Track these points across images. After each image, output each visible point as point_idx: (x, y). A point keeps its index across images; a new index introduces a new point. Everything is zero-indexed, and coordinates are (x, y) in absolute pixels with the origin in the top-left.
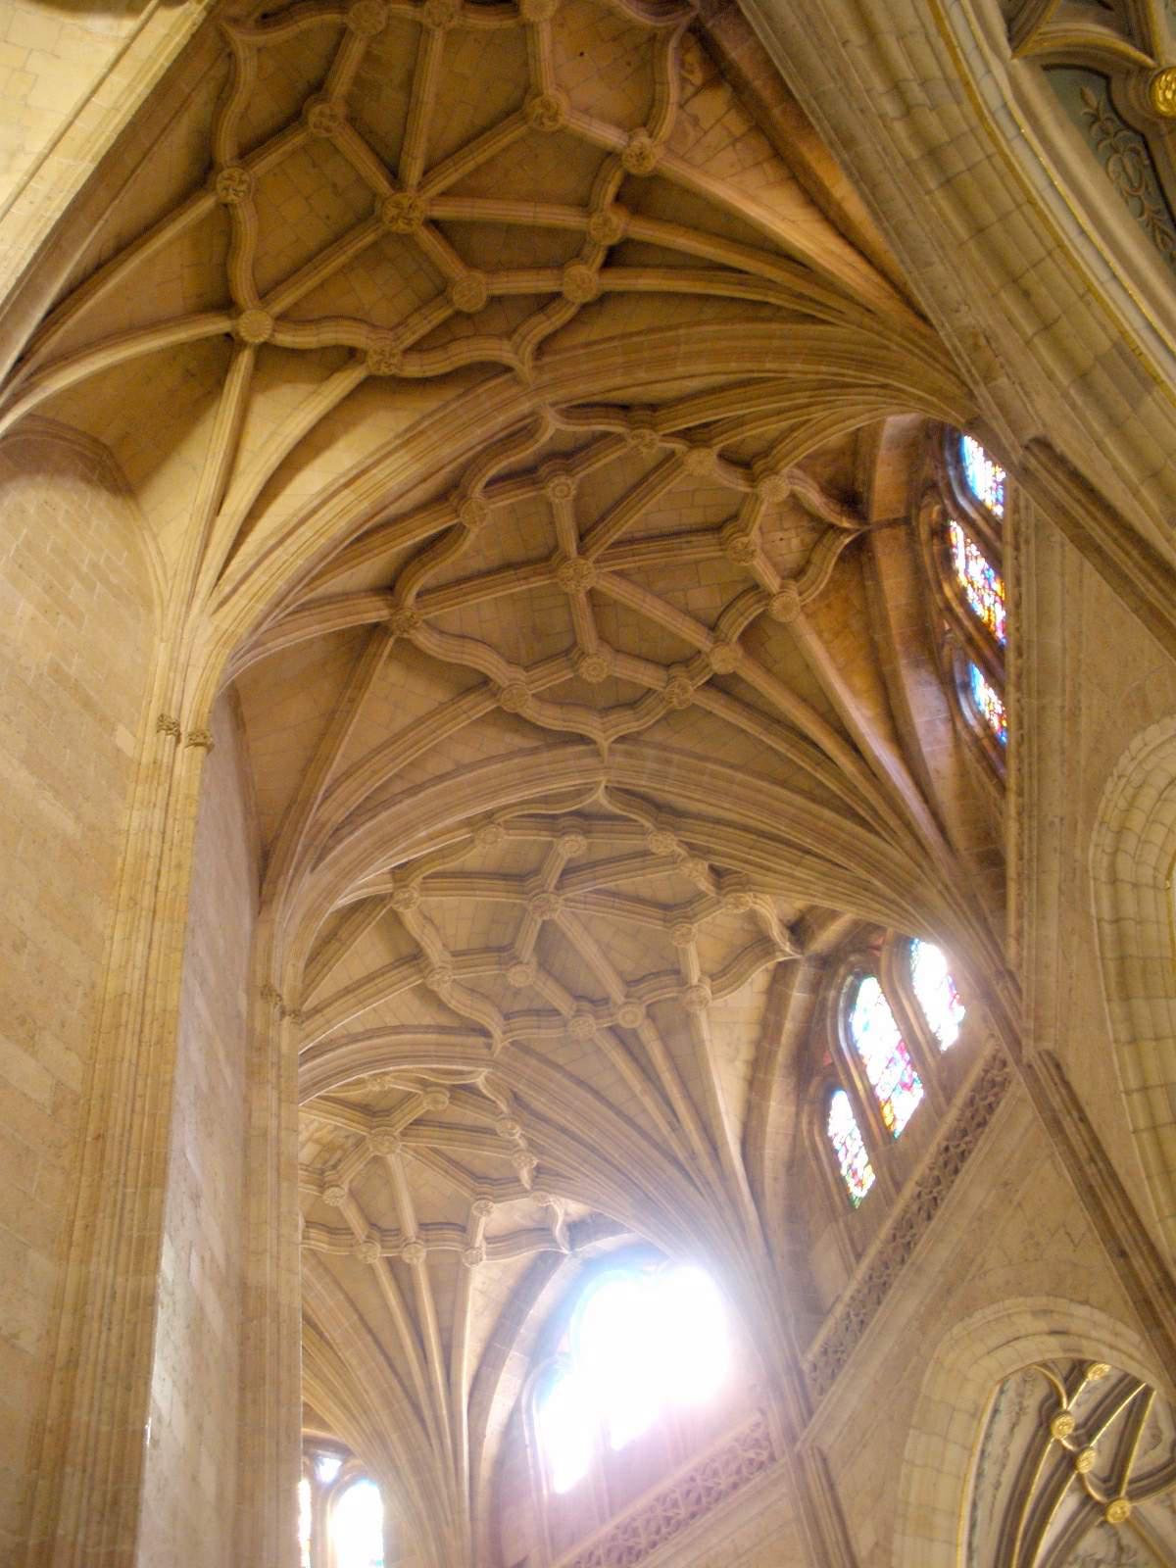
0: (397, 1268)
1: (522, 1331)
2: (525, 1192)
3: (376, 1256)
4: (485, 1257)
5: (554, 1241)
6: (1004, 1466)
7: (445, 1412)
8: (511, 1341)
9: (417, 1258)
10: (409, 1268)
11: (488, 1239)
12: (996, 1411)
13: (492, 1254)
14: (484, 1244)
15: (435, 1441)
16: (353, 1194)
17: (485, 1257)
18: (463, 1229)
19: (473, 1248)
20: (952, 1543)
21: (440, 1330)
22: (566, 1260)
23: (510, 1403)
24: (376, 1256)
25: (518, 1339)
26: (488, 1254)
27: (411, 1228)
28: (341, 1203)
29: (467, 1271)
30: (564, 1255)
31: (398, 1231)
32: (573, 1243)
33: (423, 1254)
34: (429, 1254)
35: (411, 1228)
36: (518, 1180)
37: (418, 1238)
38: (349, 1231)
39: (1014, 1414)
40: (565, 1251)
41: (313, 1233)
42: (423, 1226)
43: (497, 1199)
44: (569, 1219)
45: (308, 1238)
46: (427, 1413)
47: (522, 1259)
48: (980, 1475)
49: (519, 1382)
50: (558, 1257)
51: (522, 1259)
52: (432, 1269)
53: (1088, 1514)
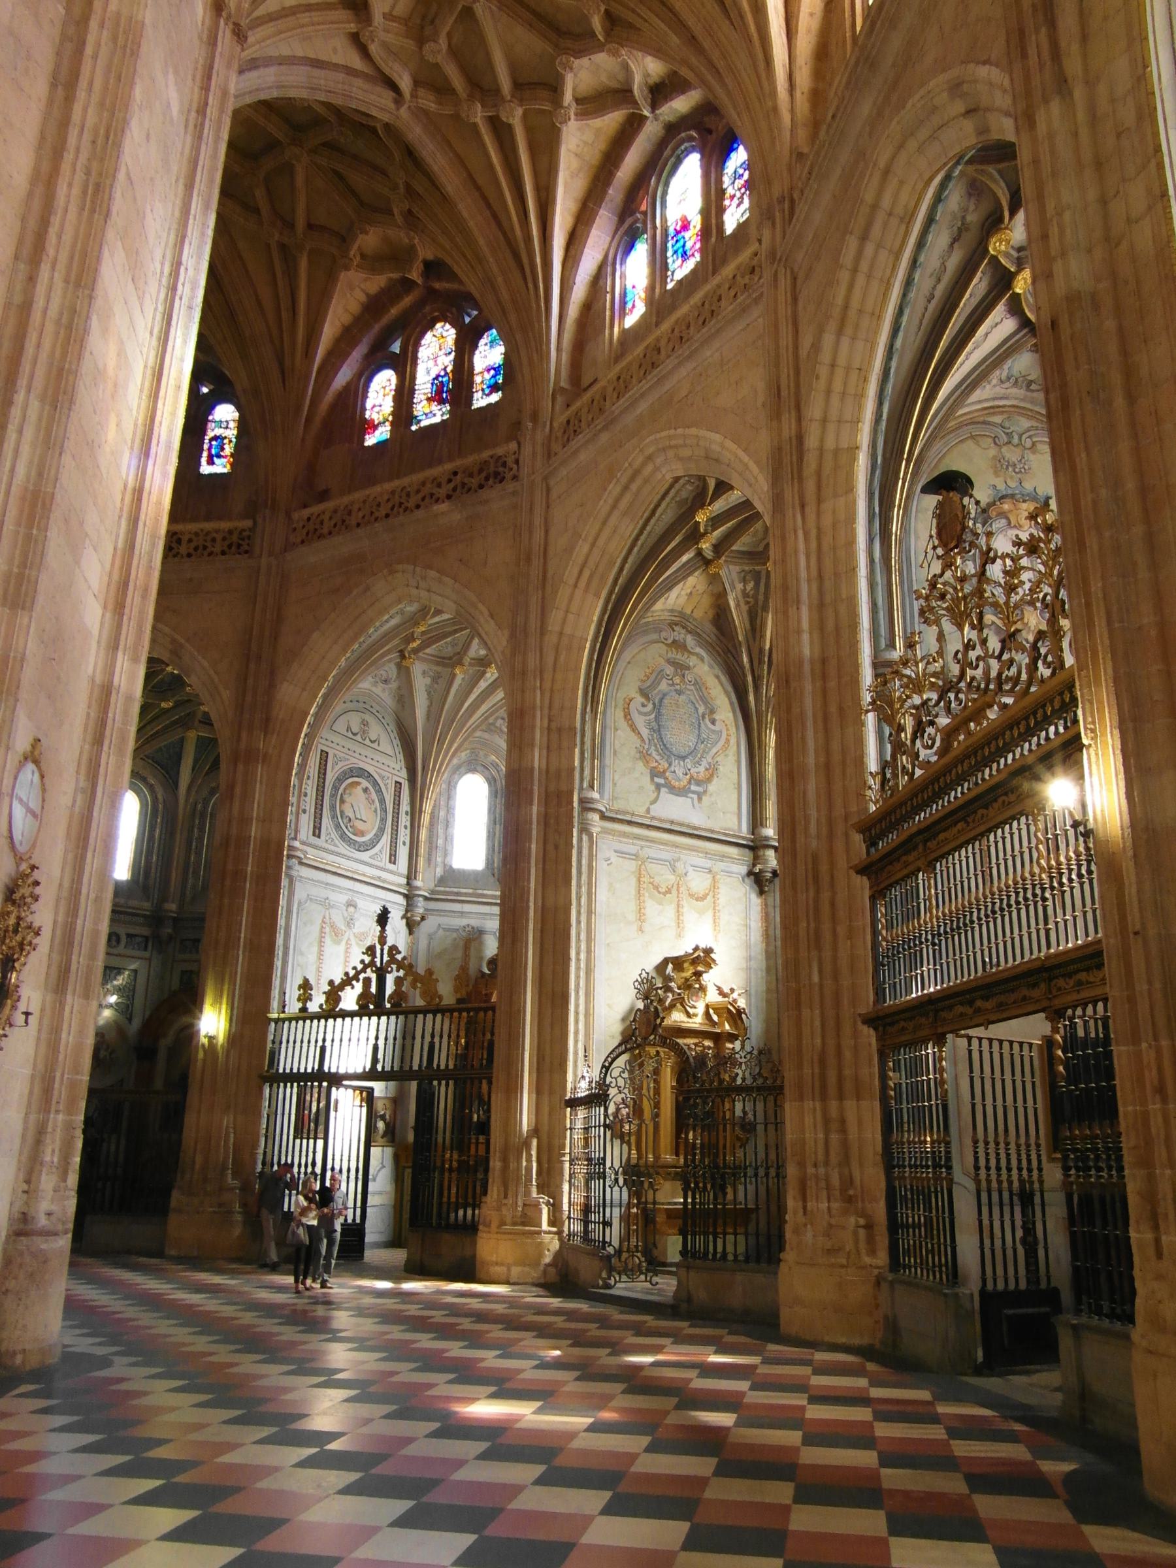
0: (501, 131)
1: (610, 192)
2: (600, 47)
3: (478, 115)
4: (573, 117)
5: (636, 103)
6: (939, 280)
7: (538, 260)
8: (602, 200)
9: (515, 117)
10: (510, 127)
11: (578, 101)
12: (930, 220)
13: (583, 115)
14: (574, 105)
15: (531, 285)
16: (453, 52)
17: (573, 117)
18: (554, 89)
19: (561, 107)
20: (873, 345)
21: (538, 189)
22: (648, 123)
23: (599, 257)
24: (478, 115)
25: (607, 199)
26: (576, 115)
27: (505, 84)
28: (439, 59)
29: (559, 130)
30: (646, 118)
31: (497, 91)
32: (654, 106)
33: (519, 112)
34: (525, 115)
35: (505, 84)
36: (593, 34)
37: (512, 96)
38: (453, 91)
39: (955, 229)
40: (646, 113)
41: (421, 92)
42: (518, 85)
43: (579, 54)
44: (651, 81)
45: (417, 97)
46: (525, 261)
47: (612, 120)
48: (908, 283)
49: (609, 239)
50: (642, 119)
51: (612, 120)
52: (529, 130)
53: (1024, 336)
